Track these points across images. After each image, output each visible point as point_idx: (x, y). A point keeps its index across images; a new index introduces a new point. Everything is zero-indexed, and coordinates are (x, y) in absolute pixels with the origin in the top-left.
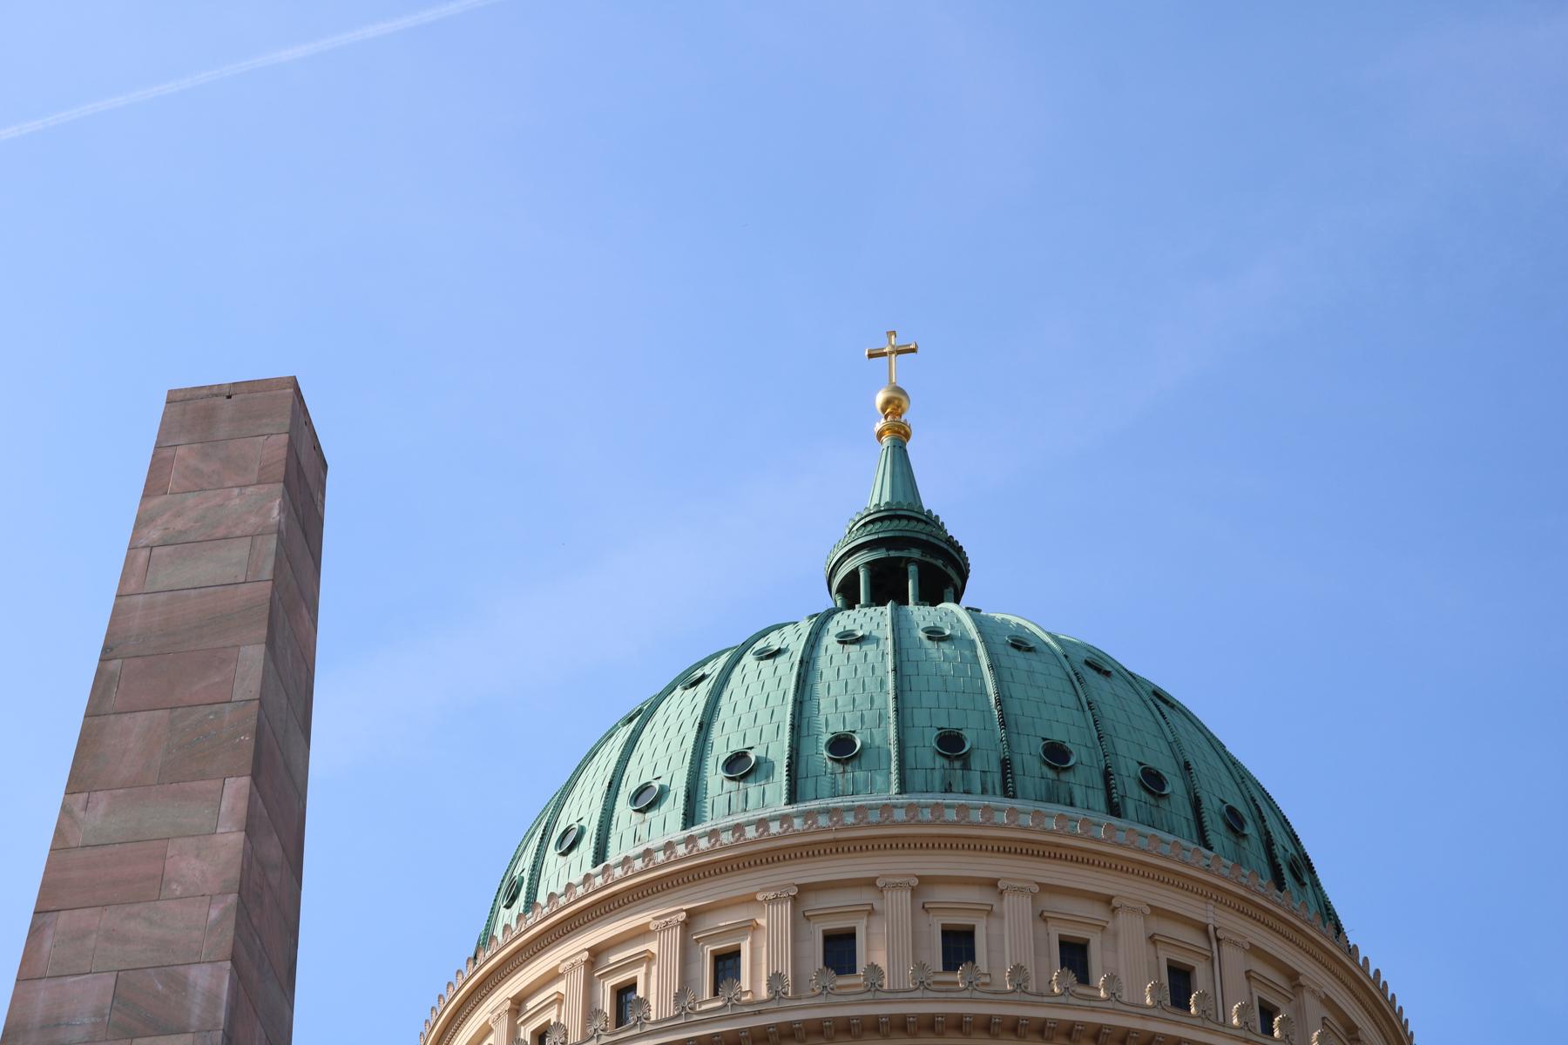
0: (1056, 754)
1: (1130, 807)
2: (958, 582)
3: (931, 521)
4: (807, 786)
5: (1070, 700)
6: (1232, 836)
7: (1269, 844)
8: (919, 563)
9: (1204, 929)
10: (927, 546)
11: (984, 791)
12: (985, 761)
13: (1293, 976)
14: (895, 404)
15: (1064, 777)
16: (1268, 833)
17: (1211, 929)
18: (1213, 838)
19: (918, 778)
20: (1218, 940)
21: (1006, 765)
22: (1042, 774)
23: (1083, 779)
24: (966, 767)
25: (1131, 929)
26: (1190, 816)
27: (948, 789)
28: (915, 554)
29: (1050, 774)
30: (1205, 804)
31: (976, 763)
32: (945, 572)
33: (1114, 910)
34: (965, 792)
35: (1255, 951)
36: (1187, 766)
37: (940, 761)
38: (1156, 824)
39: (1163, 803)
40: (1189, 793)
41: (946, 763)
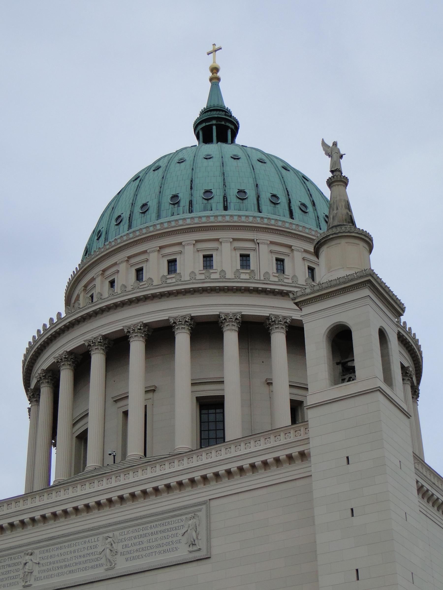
1: (232, 205)
2: (233, 127)
6: (273, 205)
8: (215, 125)
9: (253, 241)
10: (218, 119)
12: (184, 202)
13: (290, 247)
14: (215, 70)
15: (210, 201)
16: (290, 200)
17: (255, 240)
19: (163, 213)
20: (258, 243)
21: (191, 203)
22: (202, 202)
24: (179, 206)
25: (226, 248)
26: (256, 202)
27: (173, 215)
28: (214, 122)
29: (205, 202)
31: (182, 204)
32: (226, 125)
33: (221, 242)
34: (178, 215)
35: (272, 243)
36: (257, 185)
37: (172, 206)
38: (241, 209)
39: (245, 201)
40: (256, 195)
41: (173, 206)
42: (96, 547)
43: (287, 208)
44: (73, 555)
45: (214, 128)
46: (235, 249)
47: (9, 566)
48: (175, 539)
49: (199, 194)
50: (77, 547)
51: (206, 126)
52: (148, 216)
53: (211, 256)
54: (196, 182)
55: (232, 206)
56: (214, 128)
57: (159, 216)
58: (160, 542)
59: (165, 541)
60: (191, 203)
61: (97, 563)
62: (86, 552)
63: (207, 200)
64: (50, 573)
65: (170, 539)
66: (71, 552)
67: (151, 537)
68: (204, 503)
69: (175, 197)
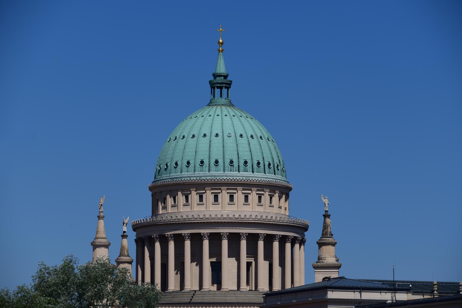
4: (212, 168)
5: (248, 149)
6: (269, 169)
7: (274, 166)
11: (236, 171)
15: (246, 167)
16: (274, 164)
18: (266, 172)
19: (226, 169)
21: (239, 166)
23: (249, 164)
24: (233, 167)
26: (263, 168)
27: (231, 171)
28: (224, 85)
29: (245, 167)
30: (265, 164)
31: (235, 166)
36: (264, 158)
43: (273, 169)
46: (257, 194)
49: (242, 162)
52: (219, 168)
53: (247, 196)
54: (240, 153)
55: (255, 170)
57: (224, 171)
60: (239, 166)
63: (246, 166)
69: (232, 162)
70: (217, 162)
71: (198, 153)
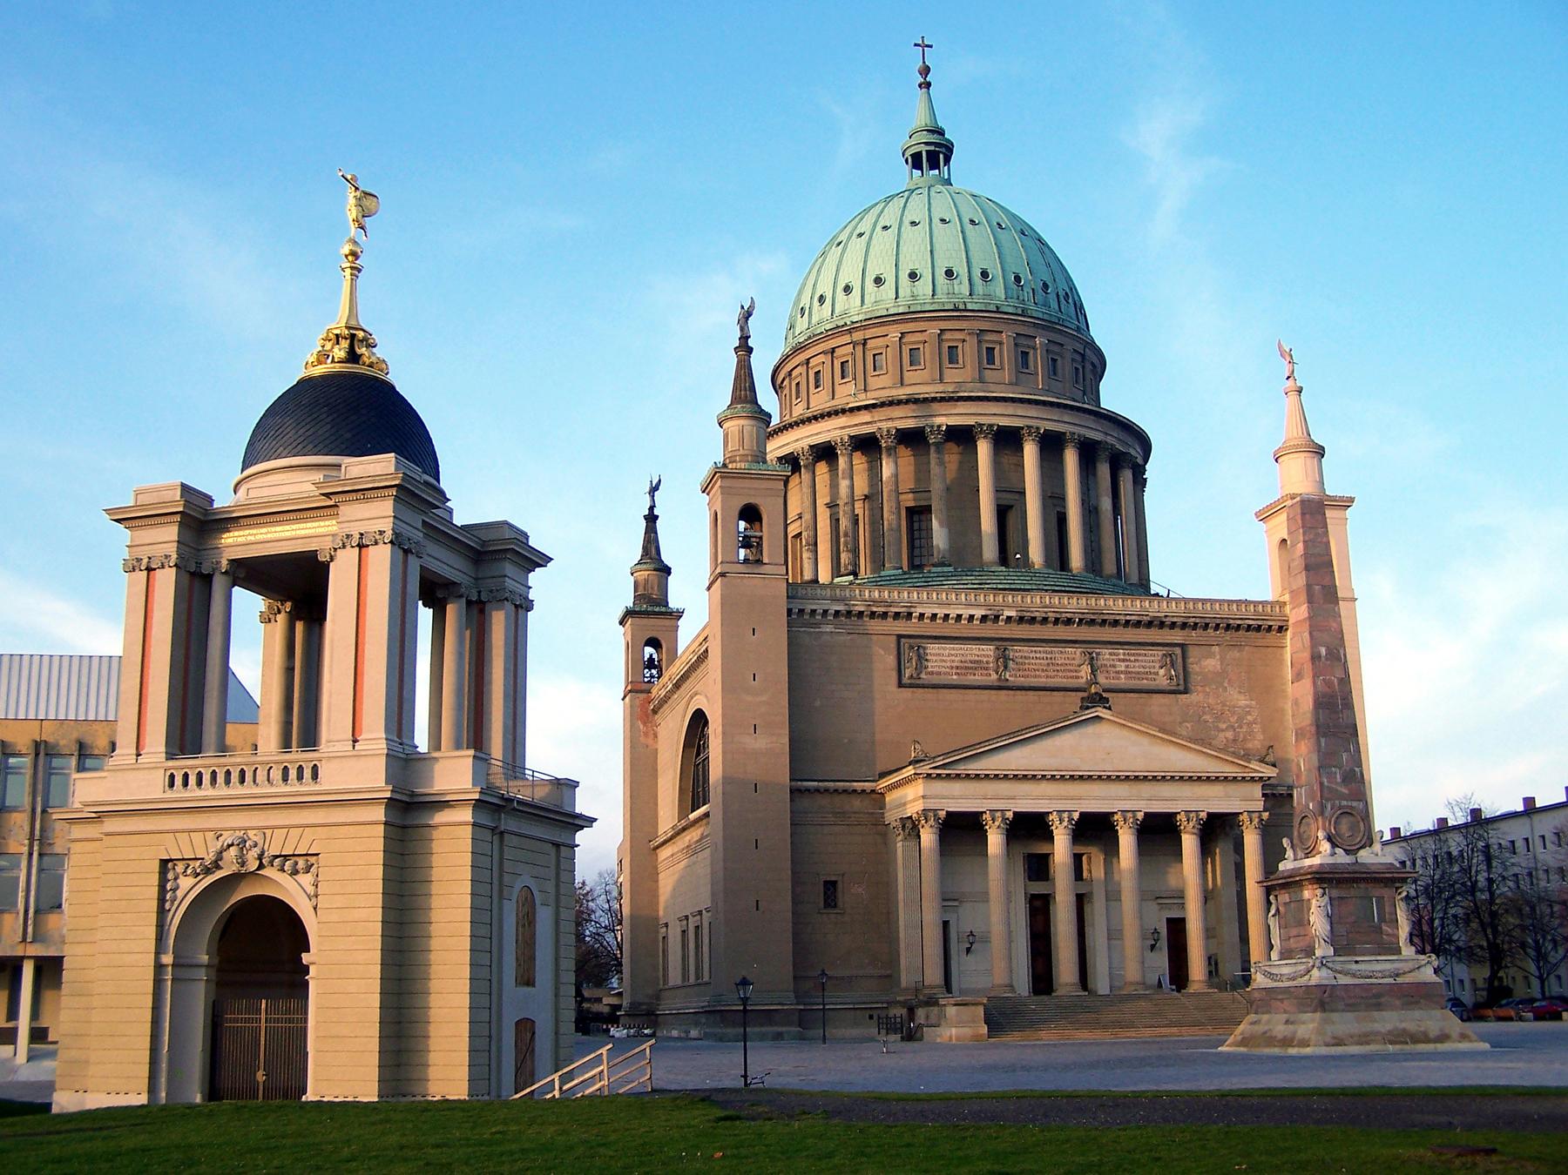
0: (1045, 286)
3: (941, 133)
24: (1022, 290)
28: (943, 150)
29: (1044, 294)
42: (1074, 659)
44: (1049, 661)
45: (941, 156)
47: (978, 656)
48: (1152, 671)
50: (1053, 656)
51: (935, 151)
56: (941, 156)
58: (1137, 669)
59: (1142, 670)
61: (1077, 674)
62: (1063, 661)
64: (1026, 673)
65: (1147, 670)
66: (1047, 658)
67: (1129, 663)
68: (1182, 646)
70: (984, 274)
71: (935, 253)
